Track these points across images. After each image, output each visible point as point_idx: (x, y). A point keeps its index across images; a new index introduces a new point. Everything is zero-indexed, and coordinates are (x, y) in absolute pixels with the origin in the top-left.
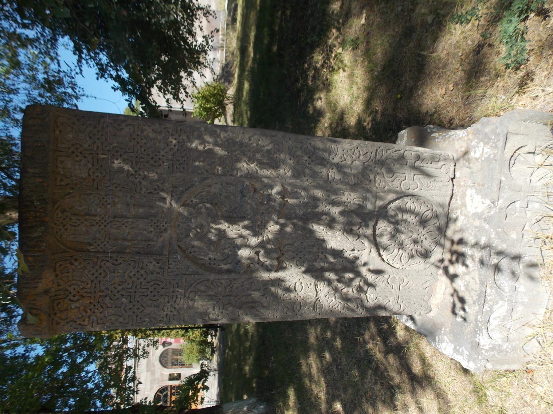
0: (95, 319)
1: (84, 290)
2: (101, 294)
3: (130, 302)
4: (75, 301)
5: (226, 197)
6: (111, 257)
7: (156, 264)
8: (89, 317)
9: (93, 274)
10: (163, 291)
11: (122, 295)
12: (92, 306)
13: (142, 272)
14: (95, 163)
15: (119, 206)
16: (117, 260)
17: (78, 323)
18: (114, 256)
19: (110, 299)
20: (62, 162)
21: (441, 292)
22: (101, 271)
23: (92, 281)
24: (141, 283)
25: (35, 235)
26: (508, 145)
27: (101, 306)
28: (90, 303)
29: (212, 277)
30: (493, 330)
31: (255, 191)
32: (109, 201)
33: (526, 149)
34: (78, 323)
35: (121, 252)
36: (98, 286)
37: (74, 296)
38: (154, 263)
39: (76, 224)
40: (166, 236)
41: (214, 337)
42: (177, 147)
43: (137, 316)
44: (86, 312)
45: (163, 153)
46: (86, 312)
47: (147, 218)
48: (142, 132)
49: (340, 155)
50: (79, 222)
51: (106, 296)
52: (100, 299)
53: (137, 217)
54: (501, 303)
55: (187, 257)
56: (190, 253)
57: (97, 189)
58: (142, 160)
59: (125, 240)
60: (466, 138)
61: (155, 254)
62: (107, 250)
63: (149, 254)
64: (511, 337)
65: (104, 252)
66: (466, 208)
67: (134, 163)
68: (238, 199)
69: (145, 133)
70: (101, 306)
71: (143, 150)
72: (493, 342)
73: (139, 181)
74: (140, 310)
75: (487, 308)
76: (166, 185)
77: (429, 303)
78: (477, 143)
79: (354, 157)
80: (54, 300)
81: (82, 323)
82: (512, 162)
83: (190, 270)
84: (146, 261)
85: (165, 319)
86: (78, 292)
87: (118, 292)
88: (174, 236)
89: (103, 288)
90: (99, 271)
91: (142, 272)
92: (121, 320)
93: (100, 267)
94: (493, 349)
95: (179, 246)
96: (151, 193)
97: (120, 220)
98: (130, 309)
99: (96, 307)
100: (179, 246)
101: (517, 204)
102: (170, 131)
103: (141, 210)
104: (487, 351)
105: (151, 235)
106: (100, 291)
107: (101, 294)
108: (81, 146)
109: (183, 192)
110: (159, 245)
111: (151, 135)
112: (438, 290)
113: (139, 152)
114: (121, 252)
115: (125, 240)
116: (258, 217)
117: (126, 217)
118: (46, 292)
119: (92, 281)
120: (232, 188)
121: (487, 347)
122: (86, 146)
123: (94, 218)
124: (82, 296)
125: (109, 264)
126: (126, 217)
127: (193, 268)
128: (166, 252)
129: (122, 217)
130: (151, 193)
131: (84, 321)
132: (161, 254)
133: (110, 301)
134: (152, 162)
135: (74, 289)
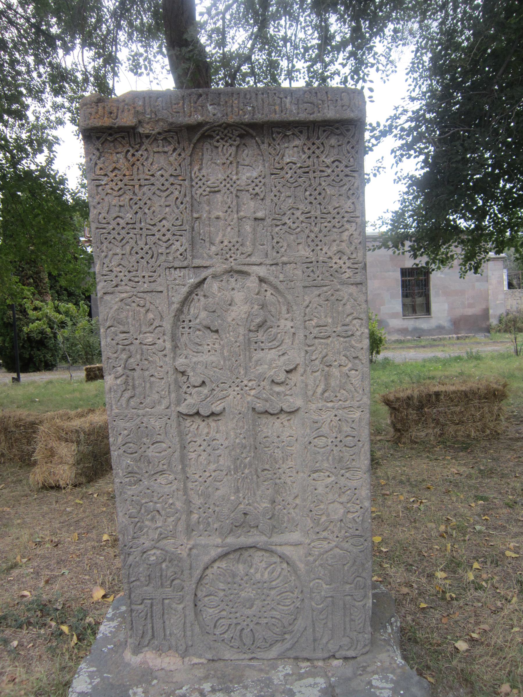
0: (103, 183)
1: (141, 168)
2: (137, 187)
3: (127, 224)
4: (126, 157)
6: (185, 196)
7: (179, 253)
8: (106, 175)
9: (162, 176)
11: (136, 213)
12: (121, 177)
14: (303, 170)
16: (182, 203)
17: (98, 162)
18: (188, 199)
19: (131, 199)
20: (301, 132)
21: (164, 665)
23: (153, 175)
24: (154, 235)
25: (210, 108)
27: (121, 189)
28: (125, 175)
29: (167, 325)
32: (257, 188)
34: (98, 162)
36: (147, 182)
37: (133, 155)
38: (182, 250)
39: (225, 151)
42: (335, 266)
43: (109, 233)
44: (112, 171)
46: (112, 171)
49: (349, 484)
50: (228, 155)
51: (134, 193)
52: (130, 187)
56: (197, 295)
57: (272, 174)
58: (313, 224)
60: (395, 665)
61: (192, 250)
62: (194, 189)
63: (192, 243)
65: (192, 186)
66: (296, 680)
67: (308, 215)
69: (347, 226)
70: (121, 189)
71: (326, 224)
73: (286, 223)
74: (117, 237)
77: (146, 649)
78: (392, 681)
79: (349, 505)
80: (128, 132)
81: (98, 167)
85: (107, 269)
86: (138, 160)
87: (140, 208)
90: (166, 183)
91: (169, 235)
93: (172, 184)
95: (205, 279)
96: (273, 238)
97: (234, 203)
98: (118, 224)
99: (119, 183)
100: (205, 279)
102: (354, 256)
106: (140, 185)
107: (137, 187)
108: (322, 152)
112: (167, 660)
113: (323, 220)
119: (153, 175)
123: (234, 173)
124: (133, 165)
125: (177, 193)
130: (273, 238)
131: (101, 169)
132: (193, 257)
133: (127, 200)
134: (313, 235)
135: (142, 155)
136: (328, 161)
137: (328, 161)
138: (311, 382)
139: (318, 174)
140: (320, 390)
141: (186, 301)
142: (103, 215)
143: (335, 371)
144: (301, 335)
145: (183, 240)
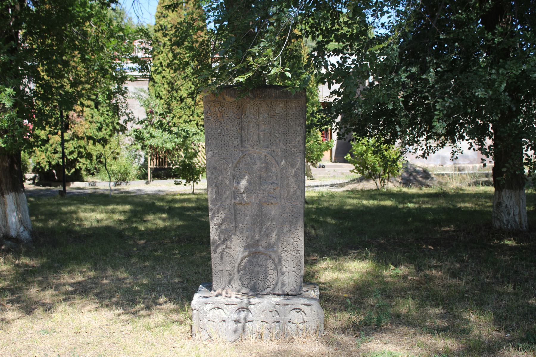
5: (270, 175)
10: (223, 148)
13: (233, 138)
15: (263, 127)
18: (240, 125)
22: (233, 120)
26: (305, 306)
30: (214, 312)
31: (274, 189)
33: (305, 317)
35: (242, 129)
38: (237, 144)
40: (250, 148)
41: (31, 182)
45: (289, 145)
47: (259, 139)
48: (298, 136)
53: (259, 135)
54: (228, 313)
55: (240, 159)
59: (248, 130)
63: (242, 141)
64: (211, 322)
68: (270, 181)
72: (208, 312)
75: (225, 306)
76: (274, 148)
82: (298, 310)
83: (234, 161)
84: (238, 140)
88: (251, 152)
89: (225, 121)
91: (233, 138)
92: (210, 130)
94: (205, 312)
101: (278, 317)
103: (262, 136)
104: (203, 309)
105: (250, 142)
109: (272, 155)
110: (246, 145)
111: (297, 139)
114: (242, 129)
115: (248, 130)
116: (262, 192)
117: (258, 130)
118: (224, 99)
120: (275, 178)
121: (205, 309)
122: (290, 112)
126: (258, 130)
127: (235, 162)
128: (243, 149)
129: (259, 128)
132: (241, 146)
134: (285, 140)
136: (292, 113)
137: (292, 113)
138: (282, 193)
139: (288, 118)
140: (285, 196)
141: (238, 162)
142: (210, 130)
143: (292, 190)
144: (279, 176)
145: (238, 140)
